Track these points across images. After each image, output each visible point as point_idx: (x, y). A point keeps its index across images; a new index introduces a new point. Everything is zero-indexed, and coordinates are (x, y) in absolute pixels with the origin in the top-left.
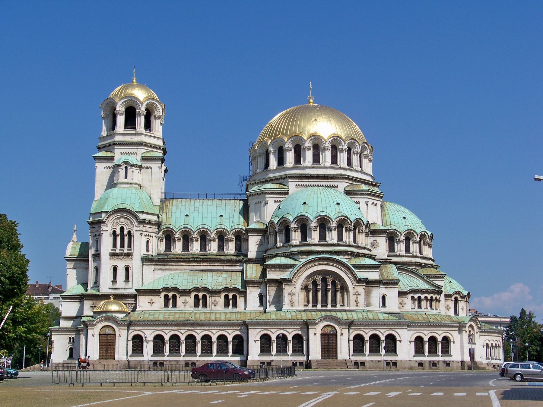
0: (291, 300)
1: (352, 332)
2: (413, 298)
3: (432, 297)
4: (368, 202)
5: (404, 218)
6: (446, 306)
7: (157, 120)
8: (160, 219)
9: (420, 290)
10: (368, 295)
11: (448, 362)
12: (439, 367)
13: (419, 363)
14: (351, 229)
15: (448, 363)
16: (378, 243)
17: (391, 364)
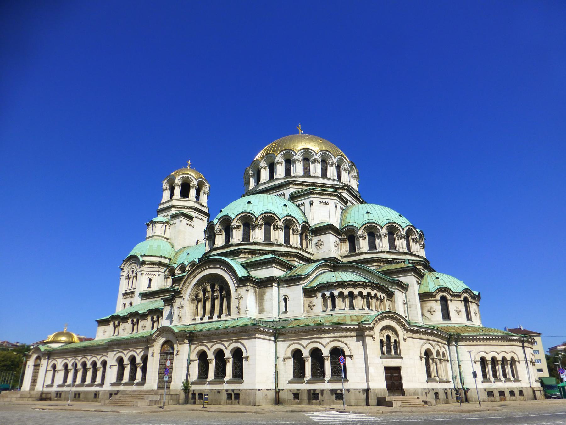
0: (179, 315)
1: (195, 348)
2: (324, 296)
3: (351, 294)
4: (313, 201)
5: (368, 213)
6: (428, 308)
7: (192, 189)
8: (172, 260)
9: (330, 284)
10: (260, 299)
11: (339, 392)
12: (323, 400)
13: (294, 394)
14: (256, 225)
15: (339, 393)
16: (323, 242)
17: (233, 396)
